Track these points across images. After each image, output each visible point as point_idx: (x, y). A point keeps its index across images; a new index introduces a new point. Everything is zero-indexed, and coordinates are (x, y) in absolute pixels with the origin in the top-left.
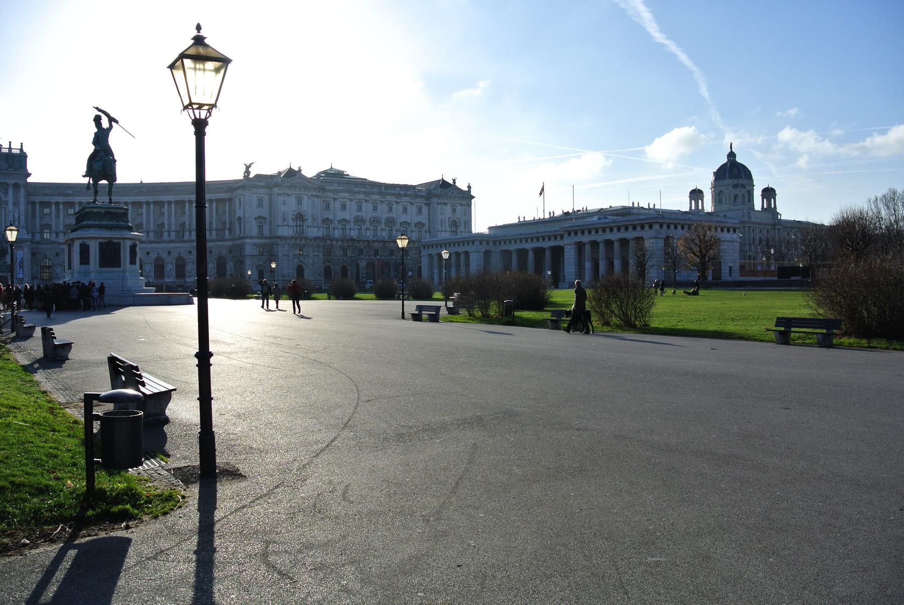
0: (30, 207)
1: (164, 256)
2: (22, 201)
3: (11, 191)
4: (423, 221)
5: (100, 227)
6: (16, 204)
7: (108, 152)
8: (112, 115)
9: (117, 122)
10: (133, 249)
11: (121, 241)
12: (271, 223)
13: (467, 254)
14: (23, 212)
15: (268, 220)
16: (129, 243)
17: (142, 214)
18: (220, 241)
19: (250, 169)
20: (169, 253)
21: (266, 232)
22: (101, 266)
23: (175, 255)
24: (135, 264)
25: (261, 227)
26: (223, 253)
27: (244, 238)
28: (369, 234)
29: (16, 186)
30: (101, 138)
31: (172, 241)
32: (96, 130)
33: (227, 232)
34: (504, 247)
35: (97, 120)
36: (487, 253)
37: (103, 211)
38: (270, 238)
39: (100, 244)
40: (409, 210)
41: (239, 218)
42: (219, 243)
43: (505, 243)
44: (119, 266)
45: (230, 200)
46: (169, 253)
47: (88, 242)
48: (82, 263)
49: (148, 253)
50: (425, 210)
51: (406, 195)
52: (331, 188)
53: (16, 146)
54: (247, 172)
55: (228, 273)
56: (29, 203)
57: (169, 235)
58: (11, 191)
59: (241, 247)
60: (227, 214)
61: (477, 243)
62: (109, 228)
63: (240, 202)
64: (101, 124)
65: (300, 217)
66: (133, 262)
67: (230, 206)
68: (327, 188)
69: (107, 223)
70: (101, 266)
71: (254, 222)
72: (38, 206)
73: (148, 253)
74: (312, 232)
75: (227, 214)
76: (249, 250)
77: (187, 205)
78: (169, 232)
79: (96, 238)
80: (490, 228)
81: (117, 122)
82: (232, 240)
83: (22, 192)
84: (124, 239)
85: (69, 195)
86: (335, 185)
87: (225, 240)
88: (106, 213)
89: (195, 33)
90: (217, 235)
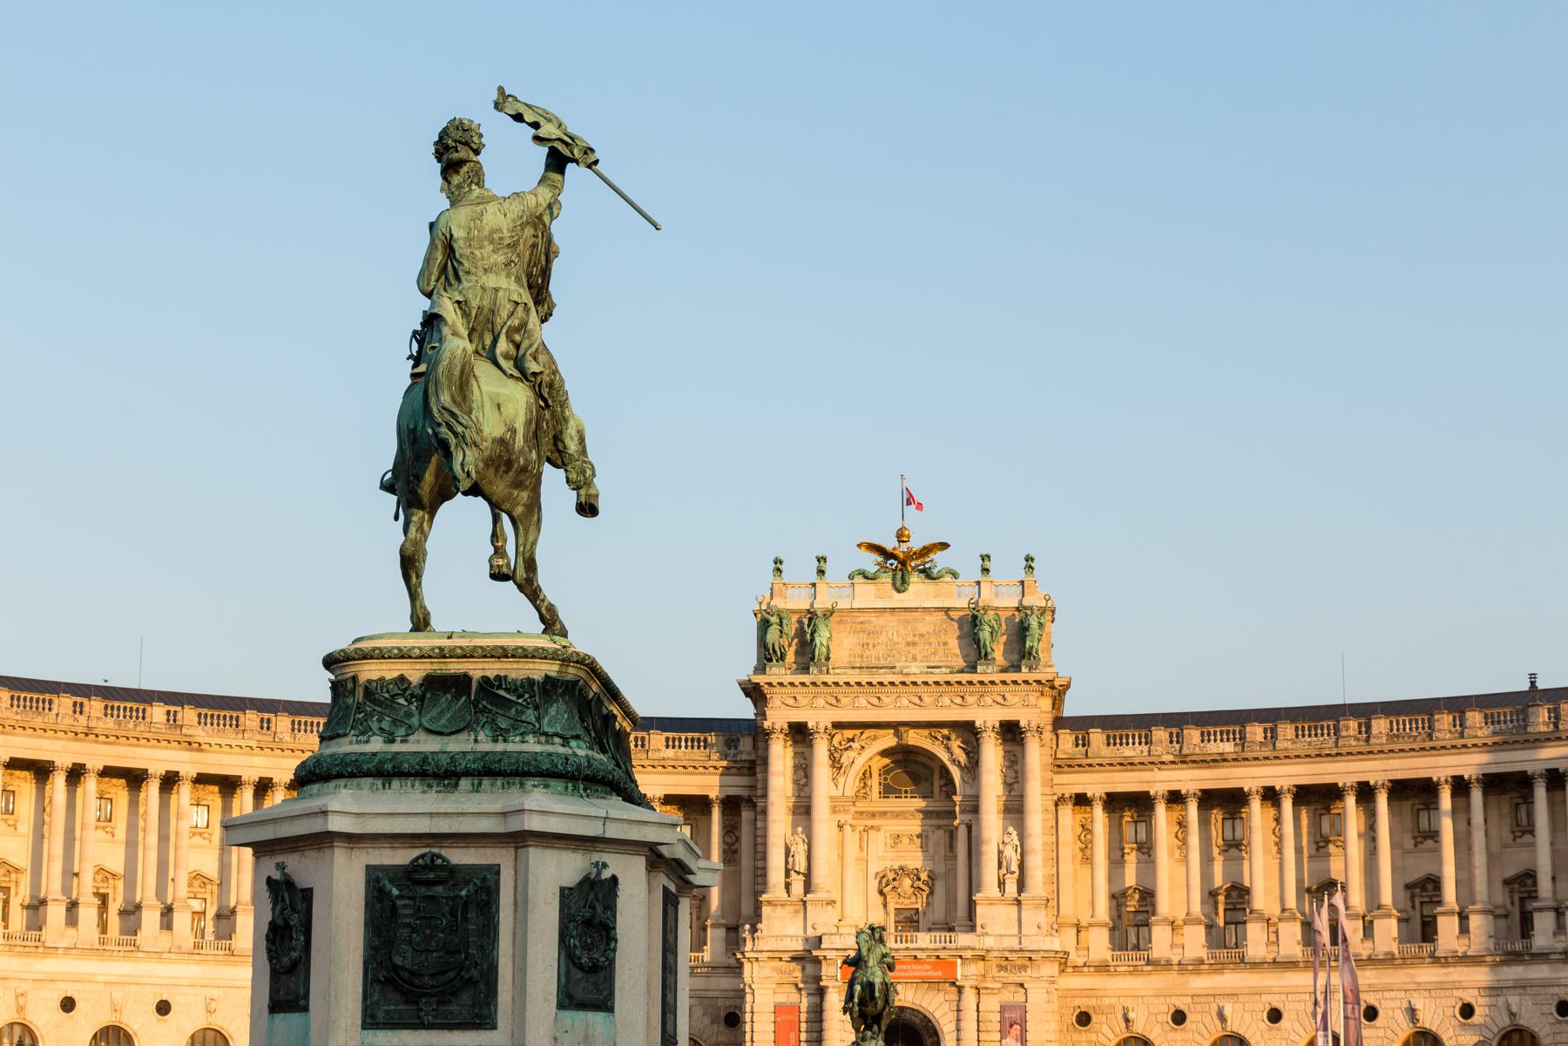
3: (992, 754)
5: (386, 772)
6: (1015, 809)
11: (501, 857)
16: (553, 873)
29: (1011, 733)
35: (455, 153)
39: (375, 877)
47: (301, 868)
58: (992, 754)
62: (443, 774)
64: (477, 177)
83: (1036, 755)
84: (520, 840)
85: (1220, 760)
88: (434, 683)
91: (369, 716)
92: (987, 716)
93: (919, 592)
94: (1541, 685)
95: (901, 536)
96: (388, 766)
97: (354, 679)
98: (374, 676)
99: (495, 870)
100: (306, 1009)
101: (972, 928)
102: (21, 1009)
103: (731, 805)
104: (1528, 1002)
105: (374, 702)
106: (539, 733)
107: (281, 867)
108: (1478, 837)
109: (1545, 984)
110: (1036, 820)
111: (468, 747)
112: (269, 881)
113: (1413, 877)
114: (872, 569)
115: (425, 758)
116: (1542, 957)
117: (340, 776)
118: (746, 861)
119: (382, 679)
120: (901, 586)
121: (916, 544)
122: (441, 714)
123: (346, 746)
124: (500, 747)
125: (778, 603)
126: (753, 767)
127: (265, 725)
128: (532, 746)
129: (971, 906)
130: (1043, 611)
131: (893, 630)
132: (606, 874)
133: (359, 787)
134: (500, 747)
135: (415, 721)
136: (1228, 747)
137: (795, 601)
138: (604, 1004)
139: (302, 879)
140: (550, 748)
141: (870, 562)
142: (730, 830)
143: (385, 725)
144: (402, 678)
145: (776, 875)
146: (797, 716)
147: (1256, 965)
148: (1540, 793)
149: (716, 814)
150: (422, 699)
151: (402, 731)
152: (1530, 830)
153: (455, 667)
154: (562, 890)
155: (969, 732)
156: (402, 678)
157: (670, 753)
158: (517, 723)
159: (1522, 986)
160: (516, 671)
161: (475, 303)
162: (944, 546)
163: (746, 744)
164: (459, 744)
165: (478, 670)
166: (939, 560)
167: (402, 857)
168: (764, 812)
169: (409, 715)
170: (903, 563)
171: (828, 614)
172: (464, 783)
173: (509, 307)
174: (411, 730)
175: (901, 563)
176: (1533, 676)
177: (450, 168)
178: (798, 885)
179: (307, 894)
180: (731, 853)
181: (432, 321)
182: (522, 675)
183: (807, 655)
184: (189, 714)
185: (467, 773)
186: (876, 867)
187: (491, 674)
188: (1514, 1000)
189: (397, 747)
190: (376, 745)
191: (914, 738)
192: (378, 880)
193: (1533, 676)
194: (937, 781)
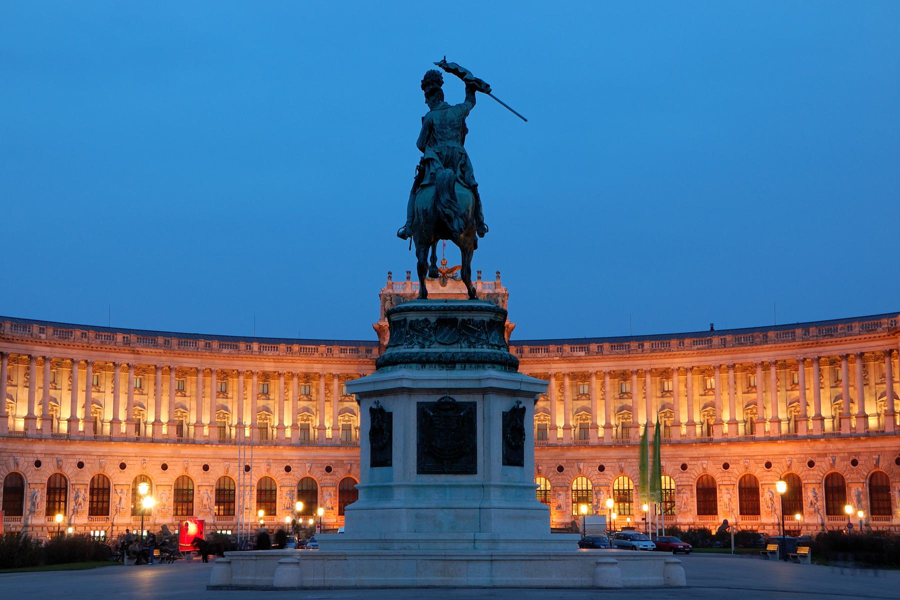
5: (423, 361)
8: (476, 74)
9: (486, 89)
11: (477, 398)
16: (500, 406)
22: (421, 470)
30: (443, 137)
32: (425, 110)
35: (432, 86)
37: (433, 319)
44: (470, 468)
46: (768, 465)
49: (726, 466)
64: (441, 96)
69: (442, 350)
70: (421, 470)
73: (726, 466)
79: (410, 391)
81: (486, 89)
85: (578, 360)
88: (441, 322)
91: (412, 336)
94: (715, 328)
96: (424, 359)
97: (405, 320)
98: (414, 319)
99: (475, 404)
100: (391, 465)
102: (60, 467)
104: (711, 463)
105: (415, 330)
106: (488, 344)
107: (377, 403)
111: (459, 350)
112: (371, 409)
115: (391, 356)
117: (401, 363)
119: (417, 320)
120: (444, 284)
122: (445, 335)
123: (402, 350)
124: (472, 350)
127: (167, 343)
128: (486, 350)
130: (504, 295)
132: (521, 406)
133: (411, 367)
134: (472, 350)
135: (433, 339)
136: (583, 354)
139: (388, 409)
140: (494, 351)
143: (420, 340)
144: (426, 320)
147: (593, 447)
150: (435, 329)
151: (428, 343)
153: (450, 315)
154: (503, 413)
156: (426, 320)
157: (343, 355)
158: (478, 340)
159: (708, 457)
160: (478, 317)
161: (445, 154)
164: (453, 349)
165: (461, 317)
167: (434, 398)
169: (430, 336)
172: (458, 366)
173: (459, 155)
174: (432, 343)
176: (712, 326)
179: (390, 415)
181: (425, 162)
182: (480, 318)
184: (133, 338)
185: (459, 362)
187: (466, 318)
189: (426, 350)
190: (416, 349)
192: (423, 409)
193: (712, 326)
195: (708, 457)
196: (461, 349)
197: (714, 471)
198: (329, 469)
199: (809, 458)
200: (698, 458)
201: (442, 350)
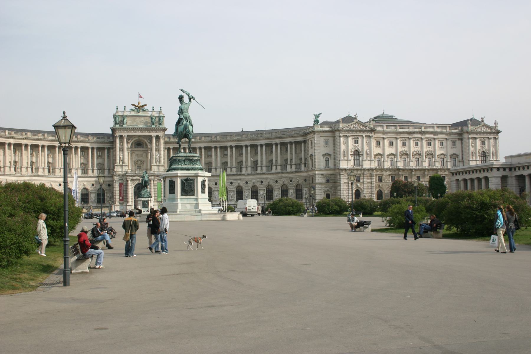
0: (166, 151)
1: (258, 184)
2: (162, 147)
3: (154, 141)
4: (457, 153)
7: (187, 119)
8: (191, 94)
10: (203, 183)
11: (195, 178)
12: (335, 158)
13: (487, 179)
14: (162, 156)
15: (332, 156)
16: (200, 179)
17: (227, 155)
18: (298, 172)
19: (319, 119)
20: (262, 182)
21: (331, 165)
22: (182, 195)
23: (265, 183)
24: (204, 193)
25: (327, 162)
26: (300, 182)
27: (315, 170)
28: (413, 165)
29: (158, 138)
31: (263, 174)
33: (303, 166)
34: (518, 173)
35: (181, 98)
36: (504, 179)
38: (334, 170)
39: (181, 180)
40: (444, 144)
41: (312, 155)
42: (297, 174)
43: (519, 169)
45: (305, 142)
46: (262, 182)
47: (174, 179)
48: (170, 193)
49: (247, 183)
50: (458, 143)
51: (442, 133)
52: (381, 130)
53: (157, 109)
54: (316, 122)
55: (304, 197)
56: (165, 149)
57: (262, 169)
58: (154, 141)
59: (313, 177)
60: (303, 152)
61: (495, 170)
63: (312, 143)
64: (183, 101)
65: (357, 153)
66: (203, 192)
67: (305, 147)
68: (378, 130)
69: (186, 166)
70: (182, 195)
71: (322, 158)
72: (172, 151)
73: (247, 183)
74: (366, 165)
75: (303, 152)
76: (319, 179)
77: (274, 147)
78: (261, 167)
80: (506, 157)
82: (306, 172)
83: (162, 141)
86: (385, 127)
87: (302, 172)
89: (63, 115)
90: (296, 168)
92: (154, 134)
93: (141, 114)
95: (139, 103)
101: (151, 170)
103: (109, 149)
108: (234, 155)
109: (244, 179)
110: (162, 152)
113: (223, 161)
114: (134, 109)
116: (244, 175)
118: (111, 158)
120: (139, 112)
121: (141, 105)
125: (117, 114)
126: (113, 142)
128: (197, 166)
129: (151, 166)
131: (138, 119)
137: (120, 114)
138: (204, 193)
141: (133, 108)
142: (109, 153)
145: (118, 161)
146: (121, 134)
148: (244, 149)
149: (106, 151)
152: (242, 154)
155: (150, 138)
159: (240, 179)
162: (146, 105)
163: (111, 138)
164: (189, 166)
166: (145, 108)
167: (185, 178)
168: (115, 150)
170: (139, 108)
171: (127, 116)
175: (139, 108)
177: (180, 101)
178: (121, 163)
180: (109, 157)
183: (122, 123)
186: (133, 160)
188: (239, 182)
190: (180, 166)
191: (141, 138)
194: (144, 145)
195: (240, 179)
196: (190, 166)
197: (242, 184)
198: (93, 185)
199: (276, 179)
200: (237, 180)
201: (186, 166)
